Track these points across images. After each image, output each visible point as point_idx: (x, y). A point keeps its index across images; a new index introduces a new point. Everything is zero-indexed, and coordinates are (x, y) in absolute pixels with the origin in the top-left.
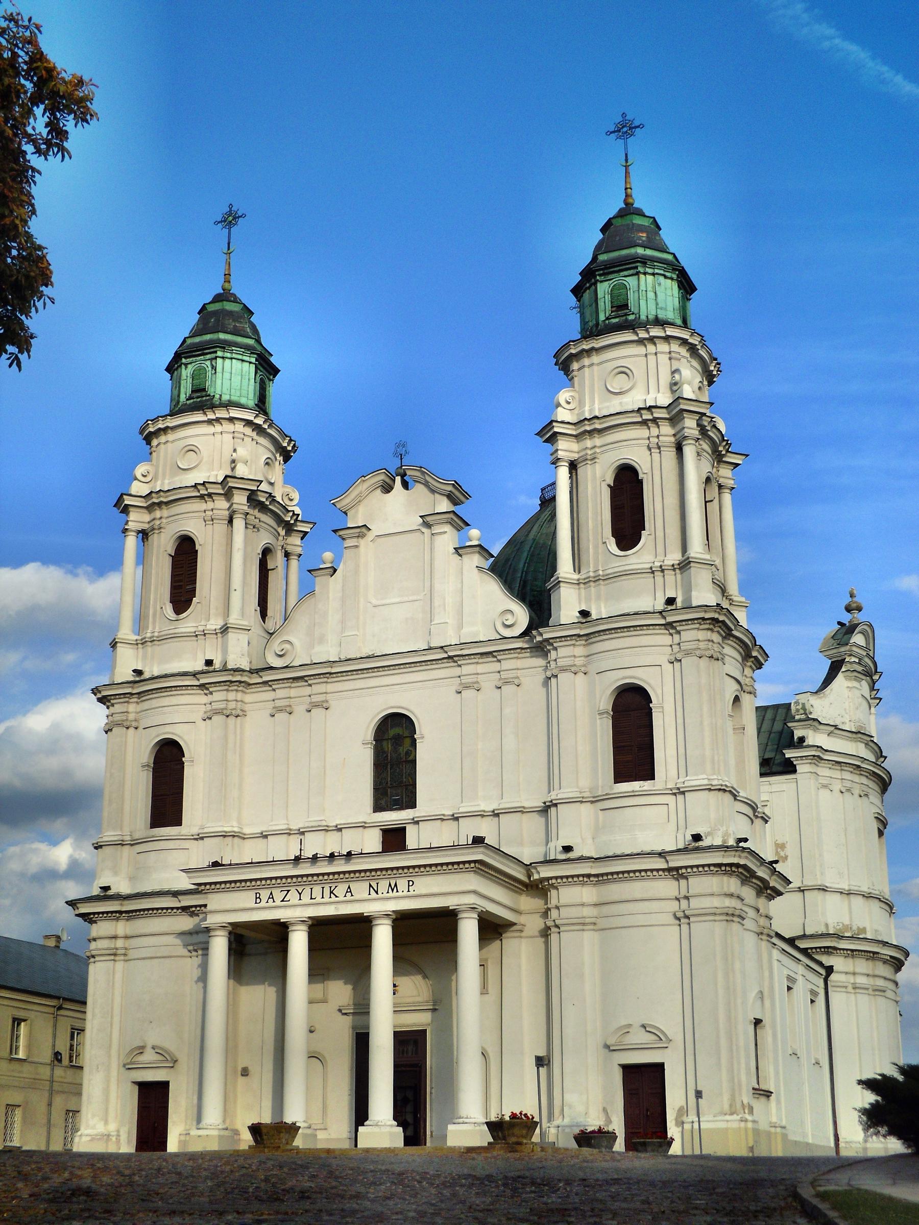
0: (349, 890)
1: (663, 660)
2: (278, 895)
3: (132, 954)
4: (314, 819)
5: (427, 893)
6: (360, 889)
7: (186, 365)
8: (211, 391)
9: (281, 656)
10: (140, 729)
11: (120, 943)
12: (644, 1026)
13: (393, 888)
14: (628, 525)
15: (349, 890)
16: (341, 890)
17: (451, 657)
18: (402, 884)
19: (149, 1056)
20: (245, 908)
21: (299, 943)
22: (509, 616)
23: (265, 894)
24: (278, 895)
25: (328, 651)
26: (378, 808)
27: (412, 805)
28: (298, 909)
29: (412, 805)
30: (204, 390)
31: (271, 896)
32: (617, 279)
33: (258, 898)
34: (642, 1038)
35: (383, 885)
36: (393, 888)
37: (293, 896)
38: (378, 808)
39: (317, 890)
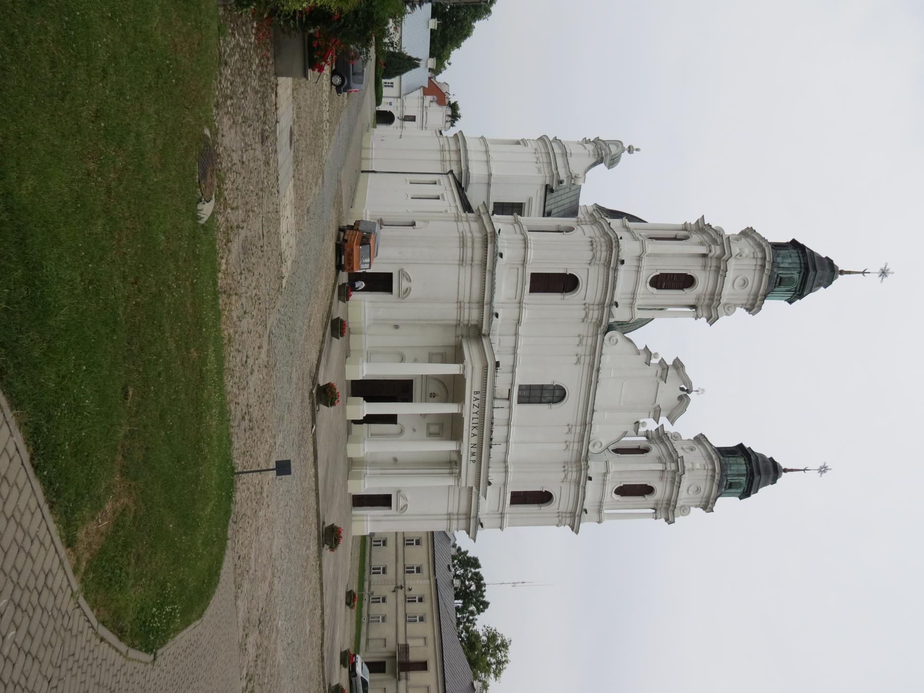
0: (475, 435)
1: (560, 510)
2: (476, 403)
3: (462, 270)
4: (520, 359)
5: (468, 468)
6: (474, 440)
7: (800, 273)
8: (777, 289)
9: (610, 339)
10: (588, 267)
11: (469, 262)
12: (406, 505)
13: (473, 454)
14: (625, 491)
15: (475, 435)
16: (475, 431)
17: (586, 424)
18: (473, 458)
19: (405, 284)
20: (472, 385)
21: (451, 408)
22: (599, 444)
23: (478, 396)
24: (476, 403)
25: (606, 360)
26: (520, 386)
27: (520, 402)
28: (469, 411)
29: (520, 402)
30: (780, 285)
31: (477, 399)
32: (744, 485)
33: (477, 393)
34: (402, 503)
35: (474, 450)
36: (473, 454)
37: (476, 409)
38: (520, 386)
39: (476, 421)
